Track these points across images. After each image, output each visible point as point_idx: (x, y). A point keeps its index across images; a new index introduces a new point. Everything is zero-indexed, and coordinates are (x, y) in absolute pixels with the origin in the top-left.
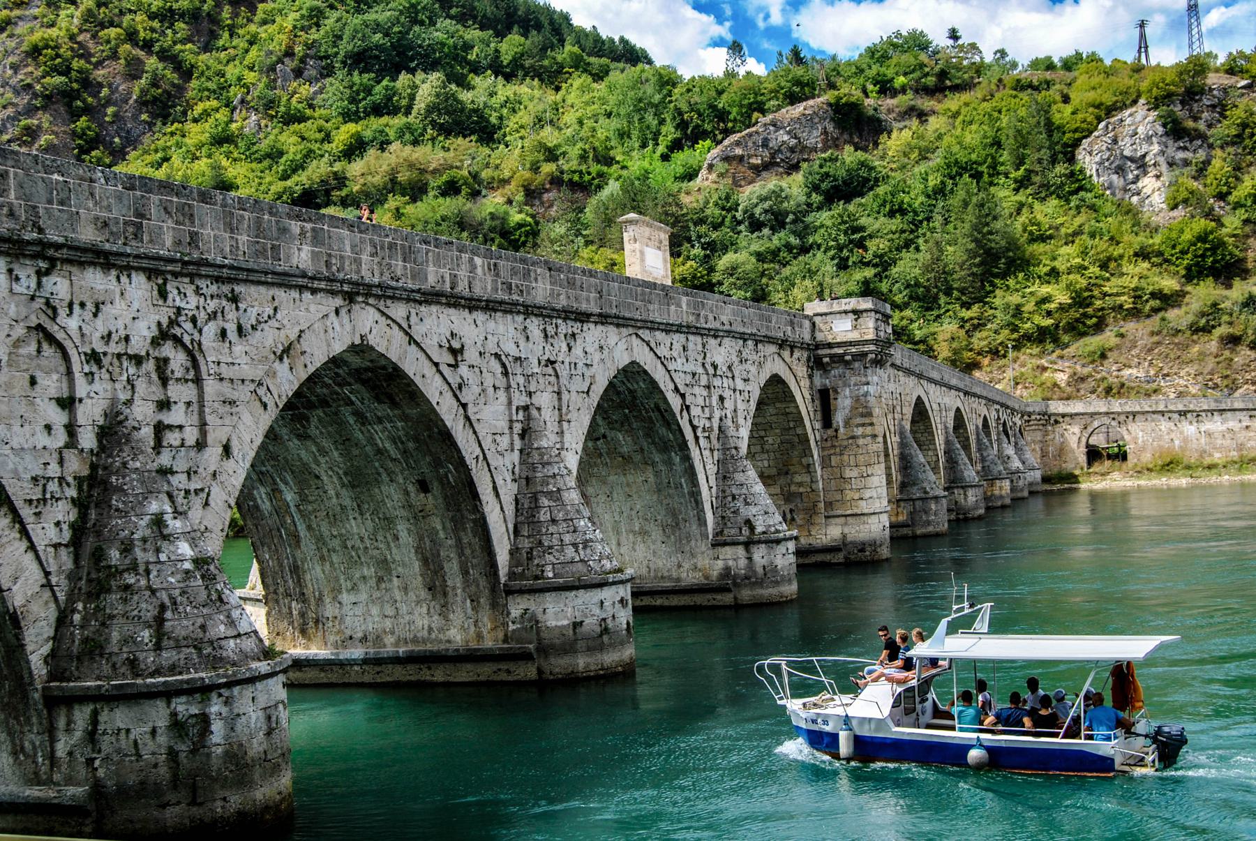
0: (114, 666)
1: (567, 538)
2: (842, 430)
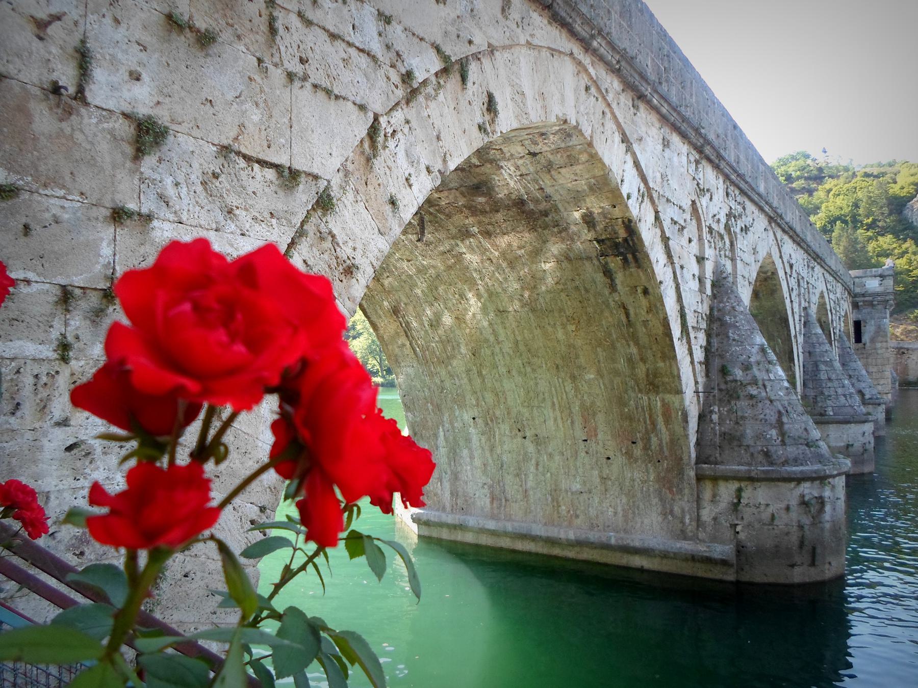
0: (752, 455)
1: (840, 391)
2: (868, 344)
